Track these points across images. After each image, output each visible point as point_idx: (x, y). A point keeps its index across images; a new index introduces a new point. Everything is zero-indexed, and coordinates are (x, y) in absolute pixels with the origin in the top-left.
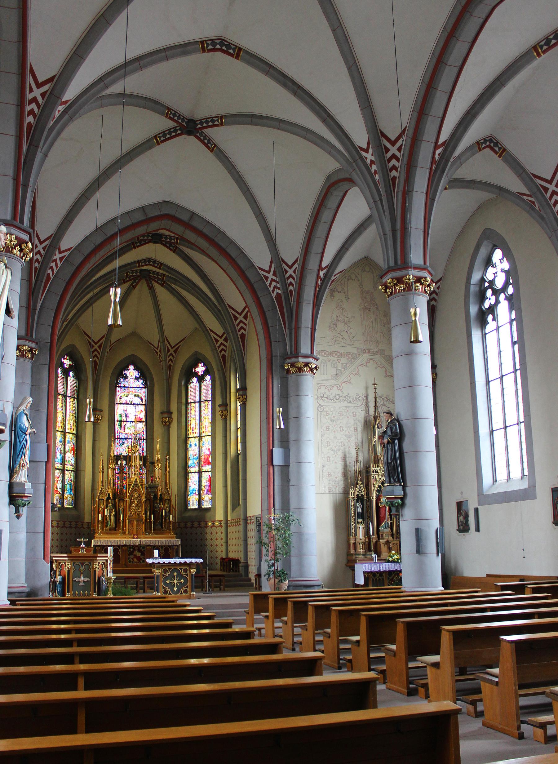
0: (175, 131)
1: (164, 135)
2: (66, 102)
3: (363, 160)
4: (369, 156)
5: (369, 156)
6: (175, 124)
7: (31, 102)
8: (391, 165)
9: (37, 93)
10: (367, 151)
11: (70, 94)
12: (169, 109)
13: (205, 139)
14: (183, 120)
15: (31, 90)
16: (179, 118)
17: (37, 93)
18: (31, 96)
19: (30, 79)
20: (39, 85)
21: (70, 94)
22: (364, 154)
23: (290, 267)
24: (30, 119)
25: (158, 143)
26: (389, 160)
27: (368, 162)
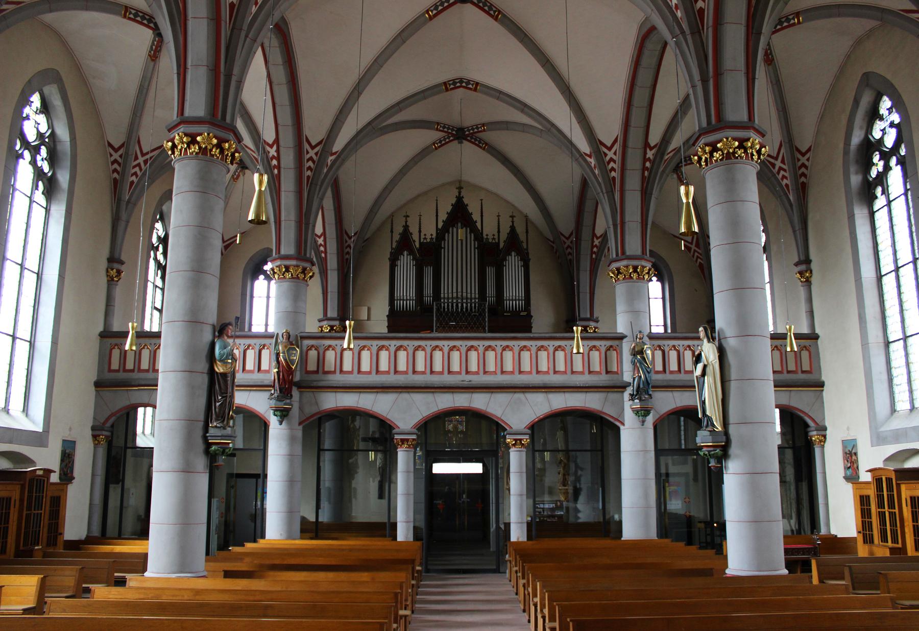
0: (445, 140)
1: (440, 142)
2: (335, 153)
3: (588, 164)
4: (592, 161)
5: (592, 161)
6: (443, 134)
7: (308, 161)
8: (610, 166)
9: (312, 153)
10: (590, 156)
11: (338, 146)
12: (438, 124)
13: (476, 140)
14: (452, 130)
15: (308, 153)
16: (448, 129)
17: (312, 153)
18: (308, 156)
19: (306, 146)
20: (313, 148)
21: (338, 146)
22: (588, 159)
23: (567, 238)
24: (309, 173)
25: (436, 148)
26: (609, 163)
27: (593, 165)
